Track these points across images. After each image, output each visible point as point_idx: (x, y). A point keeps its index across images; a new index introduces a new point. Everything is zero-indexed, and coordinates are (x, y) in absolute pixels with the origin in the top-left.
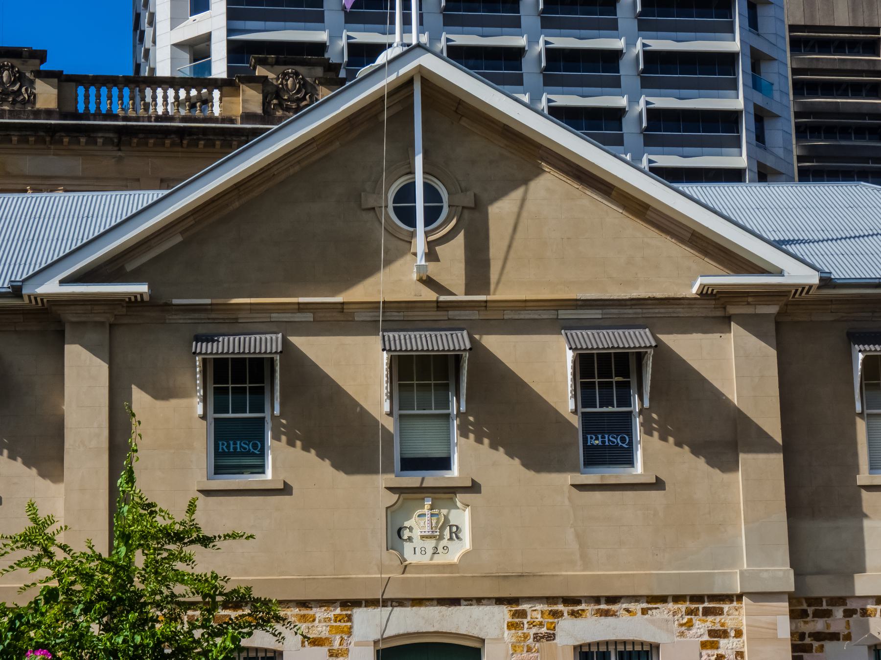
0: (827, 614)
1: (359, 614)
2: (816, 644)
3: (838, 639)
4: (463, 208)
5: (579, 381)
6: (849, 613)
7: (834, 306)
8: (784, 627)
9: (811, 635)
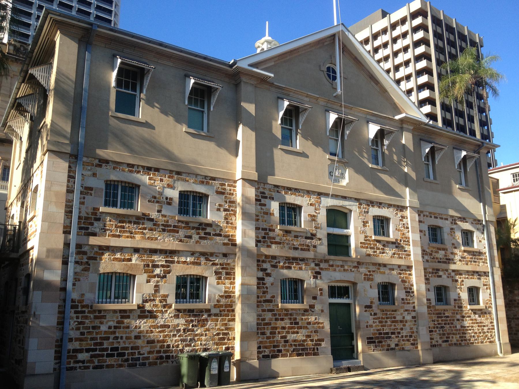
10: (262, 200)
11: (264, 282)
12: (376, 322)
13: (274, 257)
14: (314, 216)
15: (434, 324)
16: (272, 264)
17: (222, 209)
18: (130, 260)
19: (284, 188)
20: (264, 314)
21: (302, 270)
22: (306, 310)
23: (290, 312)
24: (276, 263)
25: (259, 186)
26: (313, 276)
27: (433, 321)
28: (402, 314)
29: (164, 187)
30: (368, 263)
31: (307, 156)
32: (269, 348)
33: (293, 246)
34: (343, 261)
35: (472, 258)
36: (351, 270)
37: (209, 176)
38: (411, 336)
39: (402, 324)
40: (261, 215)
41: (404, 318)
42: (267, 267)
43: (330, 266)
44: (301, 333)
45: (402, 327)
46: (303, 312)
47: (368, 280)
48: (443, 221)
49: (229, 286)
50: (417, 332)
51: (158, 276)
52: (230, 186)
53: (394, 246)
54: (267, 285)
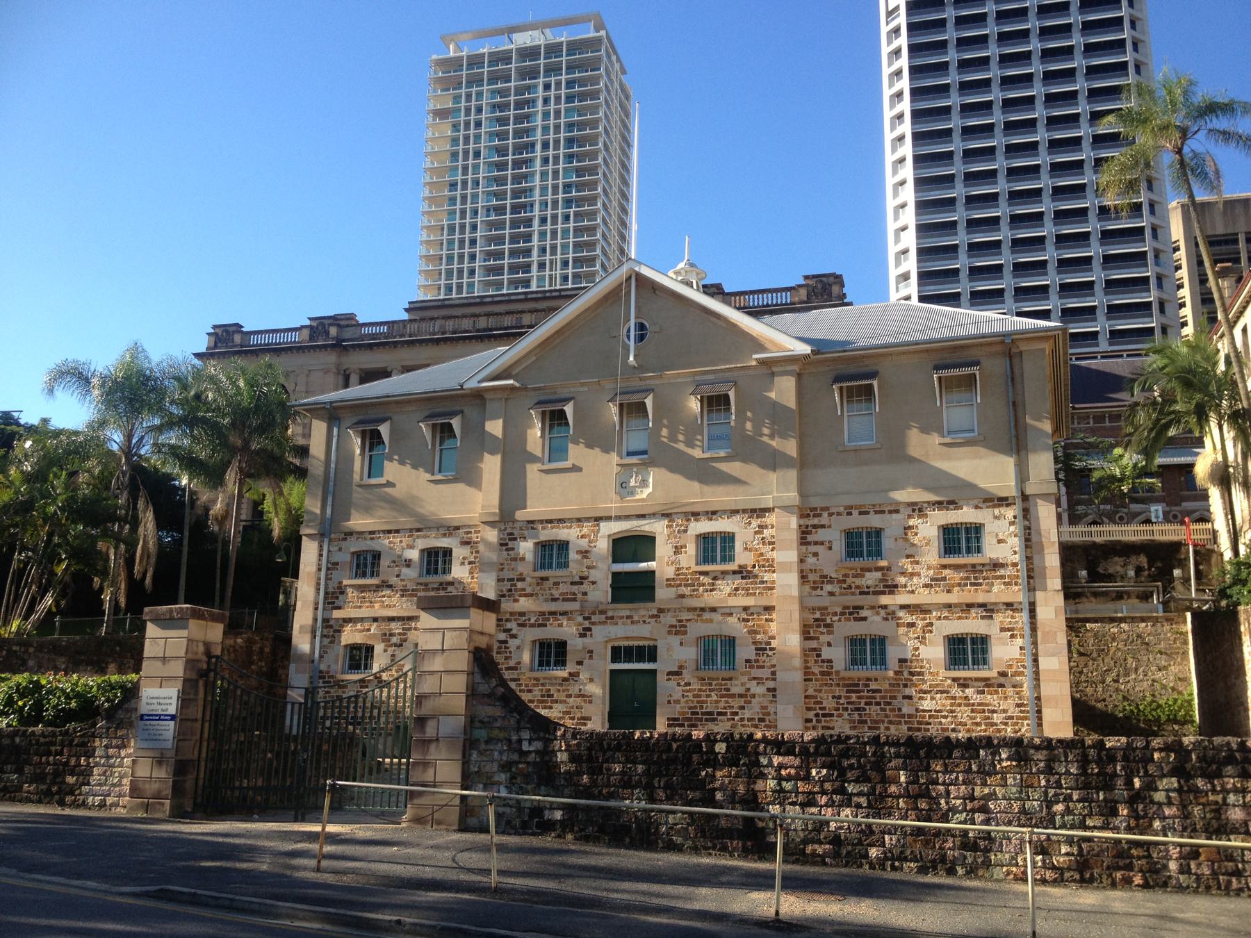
0: (819, 515)
1: (602, 524)
6: (831, 515)
8: (794, 521)
13: (522, 614)
14: (587, 552)
15: (838, 703)
17: (466, 562)
18: (369, 630)
19: (541, 522)
22: (565, 680)
23: (542, 681)
27: (834, 697)
28: (743, 684)
29: (403, 549)
31: (580, 470)
34: (631, 610)
35: (968, 578)
36: (644, 622)
41: (748, 690)
43: (607, 618)
45: (742, 704)
48: (887, 516)
51: (396, 645)
54: (511, 649)
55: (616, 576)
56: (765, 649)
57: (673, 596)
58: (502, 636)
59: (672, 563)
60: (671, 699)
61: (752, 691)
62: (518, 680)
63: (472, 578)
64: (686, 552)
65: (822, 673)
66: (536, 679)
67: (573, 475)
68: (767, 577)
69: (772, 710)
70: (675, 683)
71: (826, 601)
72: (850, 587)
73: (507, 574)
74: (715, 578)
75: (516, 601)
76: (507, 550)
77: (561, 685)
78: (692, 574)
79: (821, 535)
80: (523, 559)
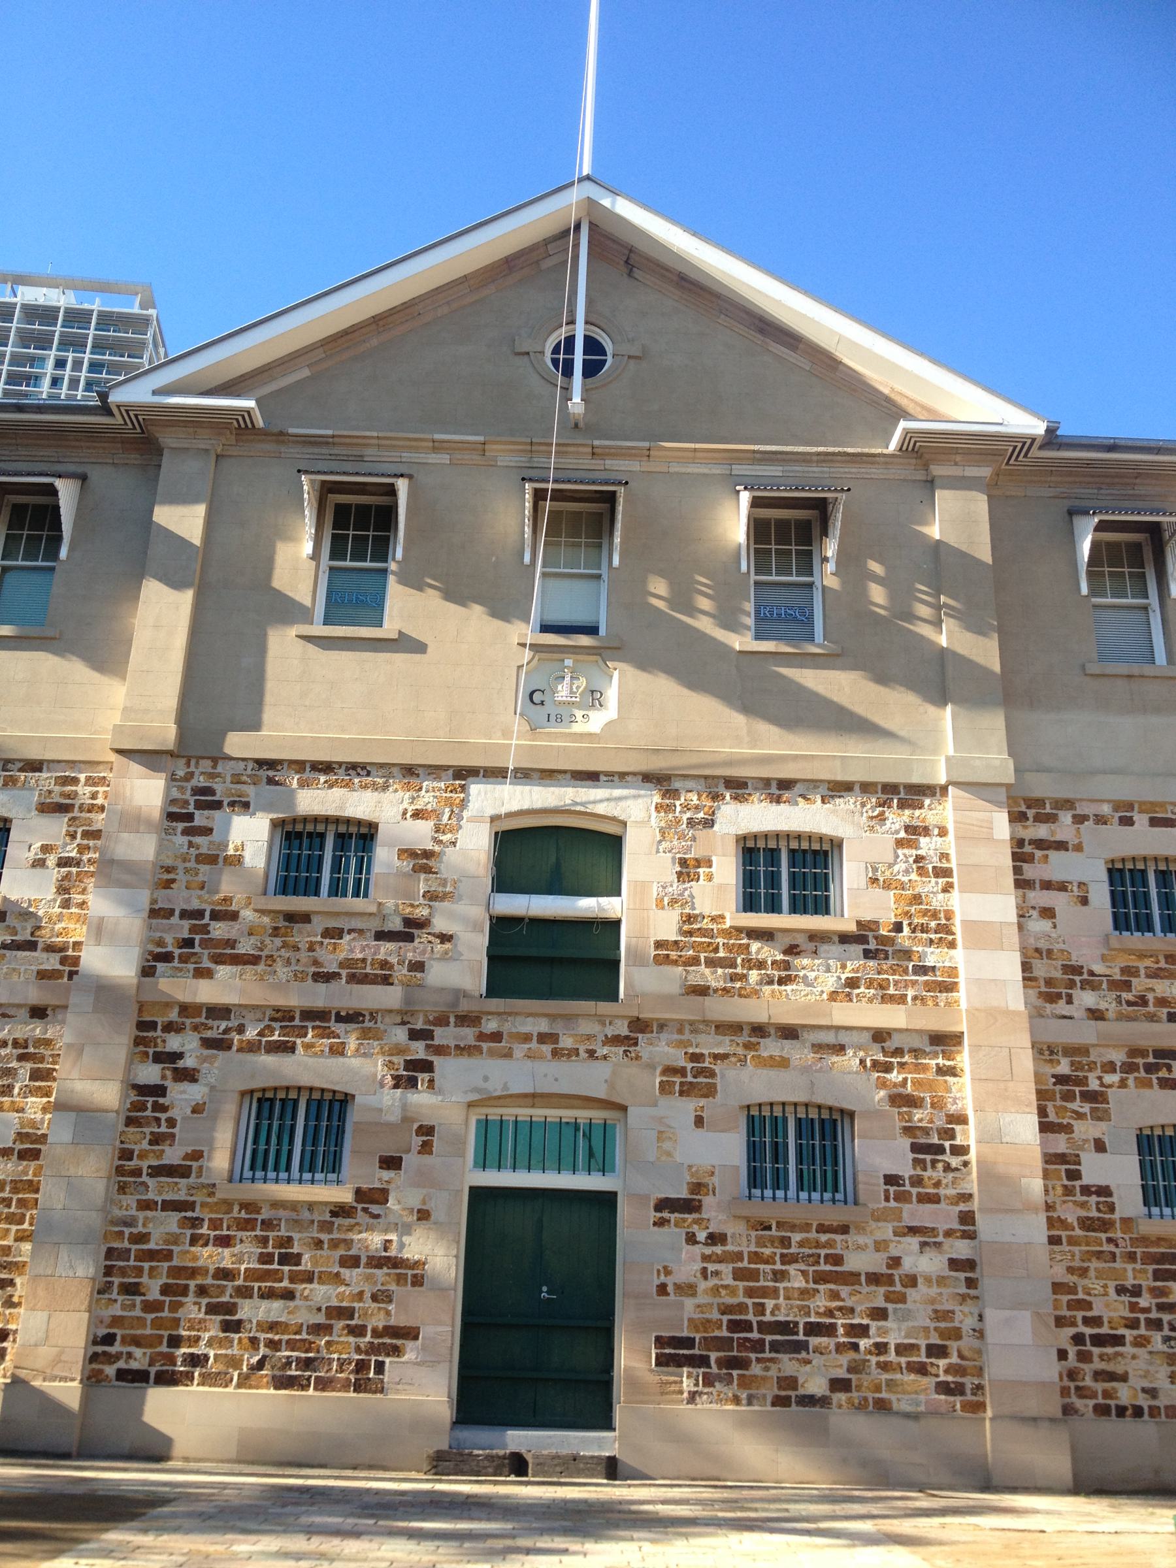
0: (1051, 819)
1: (477, 789)
2: (1038, 854)
3: (1067, 850)
4: (630, 357)
5: (752, 547)
6: (1080, 819)
7: (1053, 479)
8: (1001, 825)
9: (1031, 842)
10: (196, 817)
11: (161, 1100)
12: (716, 1273)
13: (219, 1012)
14: (428, 854)
15: (1133, 1307)
16: (209, 1034)
17: (51, 860)
19: (299, 766)
20: (146, 1218)
21: (342, 1054)
22: (340, 1211)
23: (265, 1214)
24: (227, 1031)
25: (192, 769)
26: (394, 1077)
27: (1121, 1290)
28: (880, 1246)
30: (691, 1023)
32: (151, 1346)
33: (313, 969)
34: (553, 1017)
36: (591, 1053)
37: (20, 760)
38: (936, 1351)
39: (882, 1290)
40: (188, 865)
41: (895, 1262)
42: (187, 1047)
43: (482, 1037)
44: (306, 1298)
45: (880, 1303)
46: (327, 1217)
47: (681, 1093)
49: (39, 1116)
50: (980, 1334)
52: (94, 784)
53: (859, 948)
55: (502, 926)
56: (940, 1150)
57: (675, 989)
58: (150, 1073)
59: (673, 902)
60: (670, 1281)
61: (908, 1265)
62: (190, 1206)
63: (66, 904)
64: (710, 878)
65: (1087, 1224)
66: (246, 1206)
67: (400, 659)
68: (933, 957)
69: (967, 1323)
70: (682, 1233)
71: (1086, 1033)
72: (1142, 1001)
73: (181, 898)
74: (792, 950)
75: (203, 973)
76: (186, 832)
77: (326, 1227)
78: (727, 933)
79: (1057, 866)
80: (238, 860)
